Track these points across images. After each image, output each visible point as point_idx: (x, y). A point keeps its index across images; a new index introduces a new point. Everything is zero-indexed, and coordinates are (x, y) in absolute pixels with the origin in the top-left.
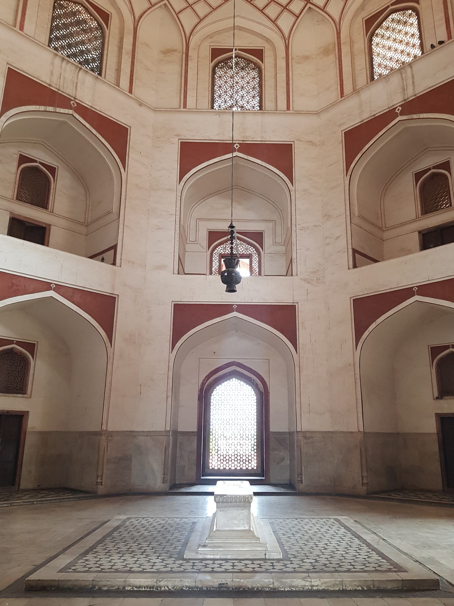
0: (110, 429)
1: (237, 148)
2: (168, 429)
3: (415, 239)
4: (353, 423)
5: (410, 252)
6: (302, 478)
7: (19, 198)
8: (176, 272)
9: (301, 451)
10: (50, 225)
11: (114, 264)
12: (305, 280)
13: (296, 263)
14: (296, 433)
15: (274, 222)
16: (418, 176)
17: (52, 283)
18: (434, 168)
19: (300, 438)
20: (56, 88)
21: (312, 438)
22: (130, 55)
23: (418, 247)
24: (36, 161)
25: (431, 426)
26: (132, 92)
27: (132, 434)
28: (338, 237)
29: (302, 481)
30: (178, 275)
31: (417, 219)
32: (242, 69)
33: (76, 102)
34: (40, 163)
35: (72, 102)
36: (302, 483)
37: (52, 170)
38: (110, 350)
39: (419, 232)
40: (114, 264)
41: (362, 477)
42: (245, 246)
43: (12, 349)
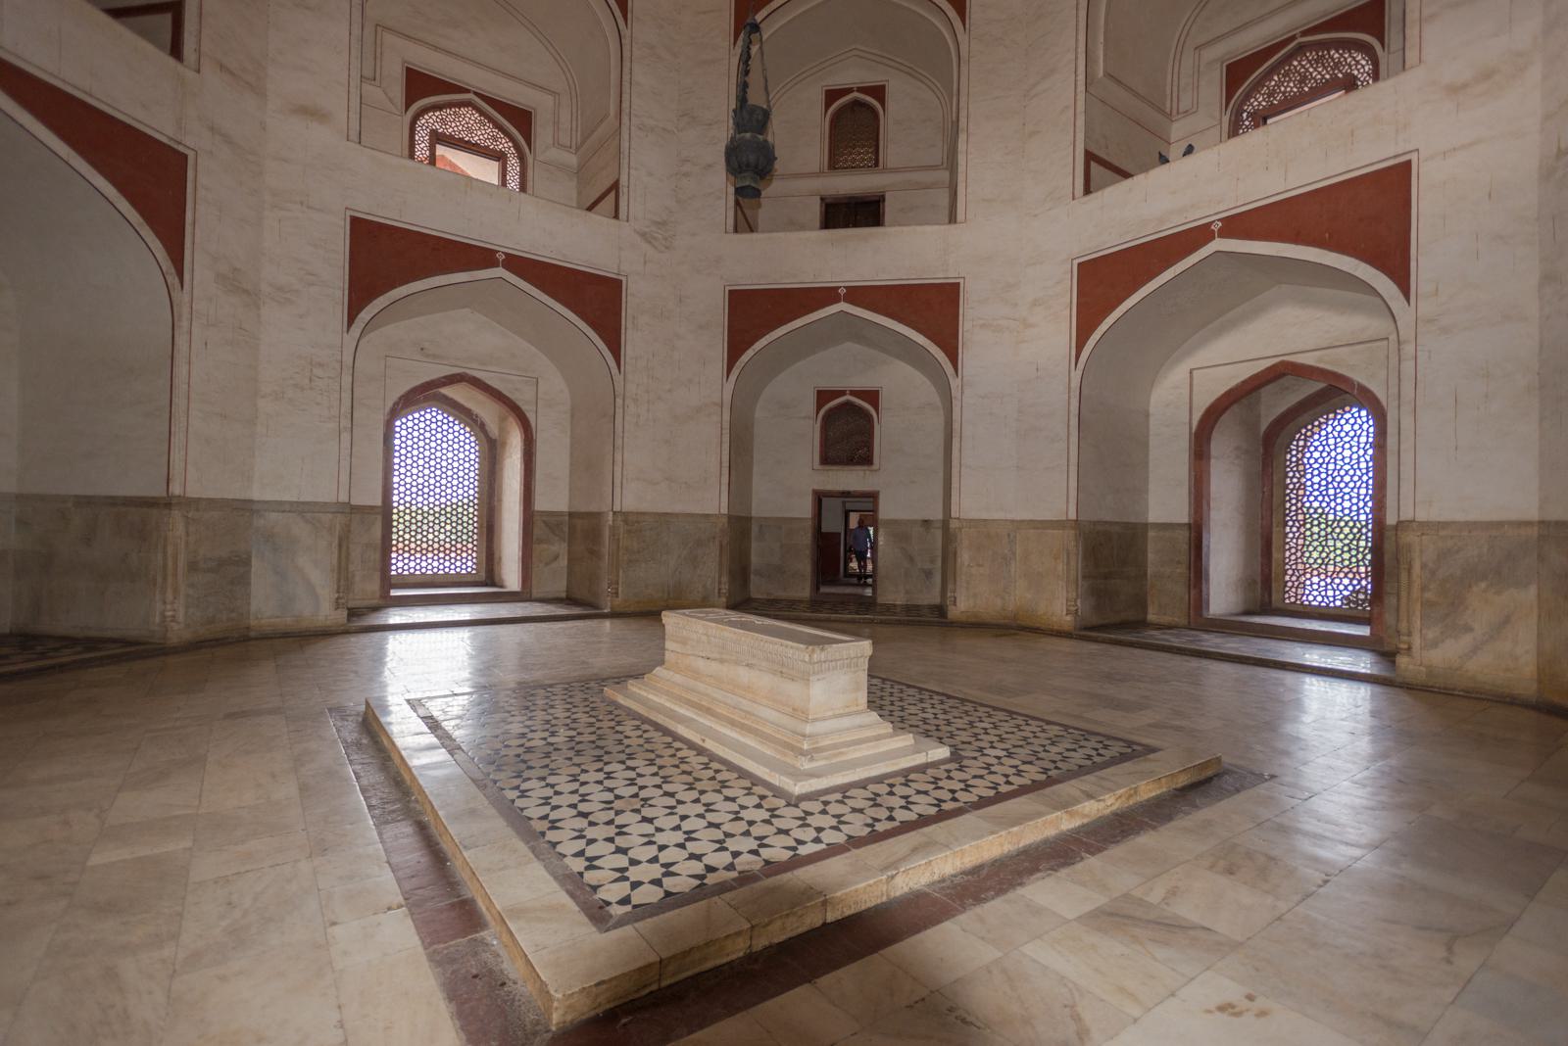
0: (188, 495)
2: (343, 498)
3: (815, 210)
4: (714, 501)
5: (802, 228)
6: (617, 589)
9: (618, 547)
12: (643, 235)
13: (626, 197)
14: (611, 513)
16: (832, 95)
18: (861, 90)
19: (619, 522)
21: (638, 522)
23: (818, 224)
25: (804, 509)
27: (246, 508)
28: (710, 166)
29: (617, 593)
31: (819, 174)
36: (617, 597)
39: (822, 199)
41: (720, 583)
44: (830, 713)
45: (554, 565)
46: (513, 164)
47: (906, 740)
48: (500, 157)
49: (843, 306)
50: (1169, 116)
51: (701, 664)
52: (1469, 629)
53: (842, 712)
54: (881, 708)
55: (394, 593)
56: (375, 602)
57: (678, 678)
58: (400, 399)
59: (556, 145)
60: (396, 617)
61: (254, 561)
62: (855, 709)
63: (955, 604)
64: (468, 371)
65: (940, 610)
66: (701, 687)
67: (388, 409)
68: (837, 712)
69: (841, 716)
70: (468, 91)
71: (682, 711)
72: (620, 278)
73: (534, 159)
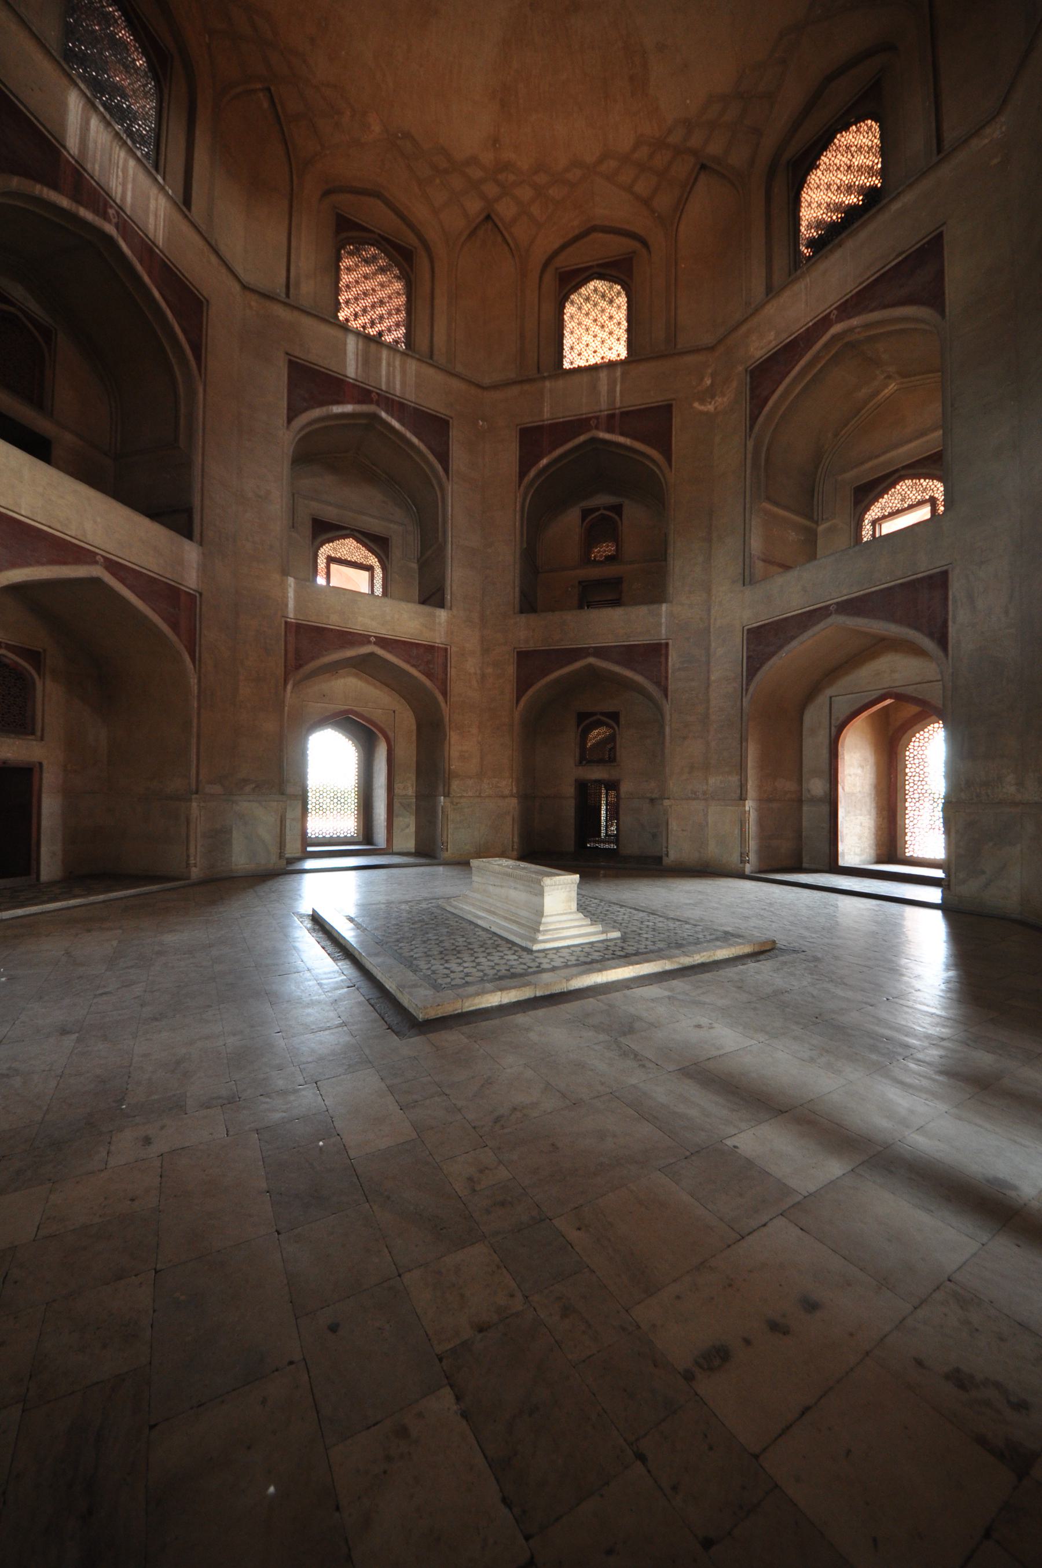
18: (605, 508)
32: (382, 270)
45: (407, 831)
46: (378, 573)
47: (599, 928)
48: (369, 568)
49: (591, 660)
50: (817, 523)
51: (491, 888)
52: (983, 872)
54: (603, 920)
55: (310, 849)
56: (298, 855)
57: (479, 896)
60: (309, 864)
61: (234, 832)
63: (667, 855)
64: (355, 708)
65: (659, 860)
66: (491, 901)
71: (480, 913)
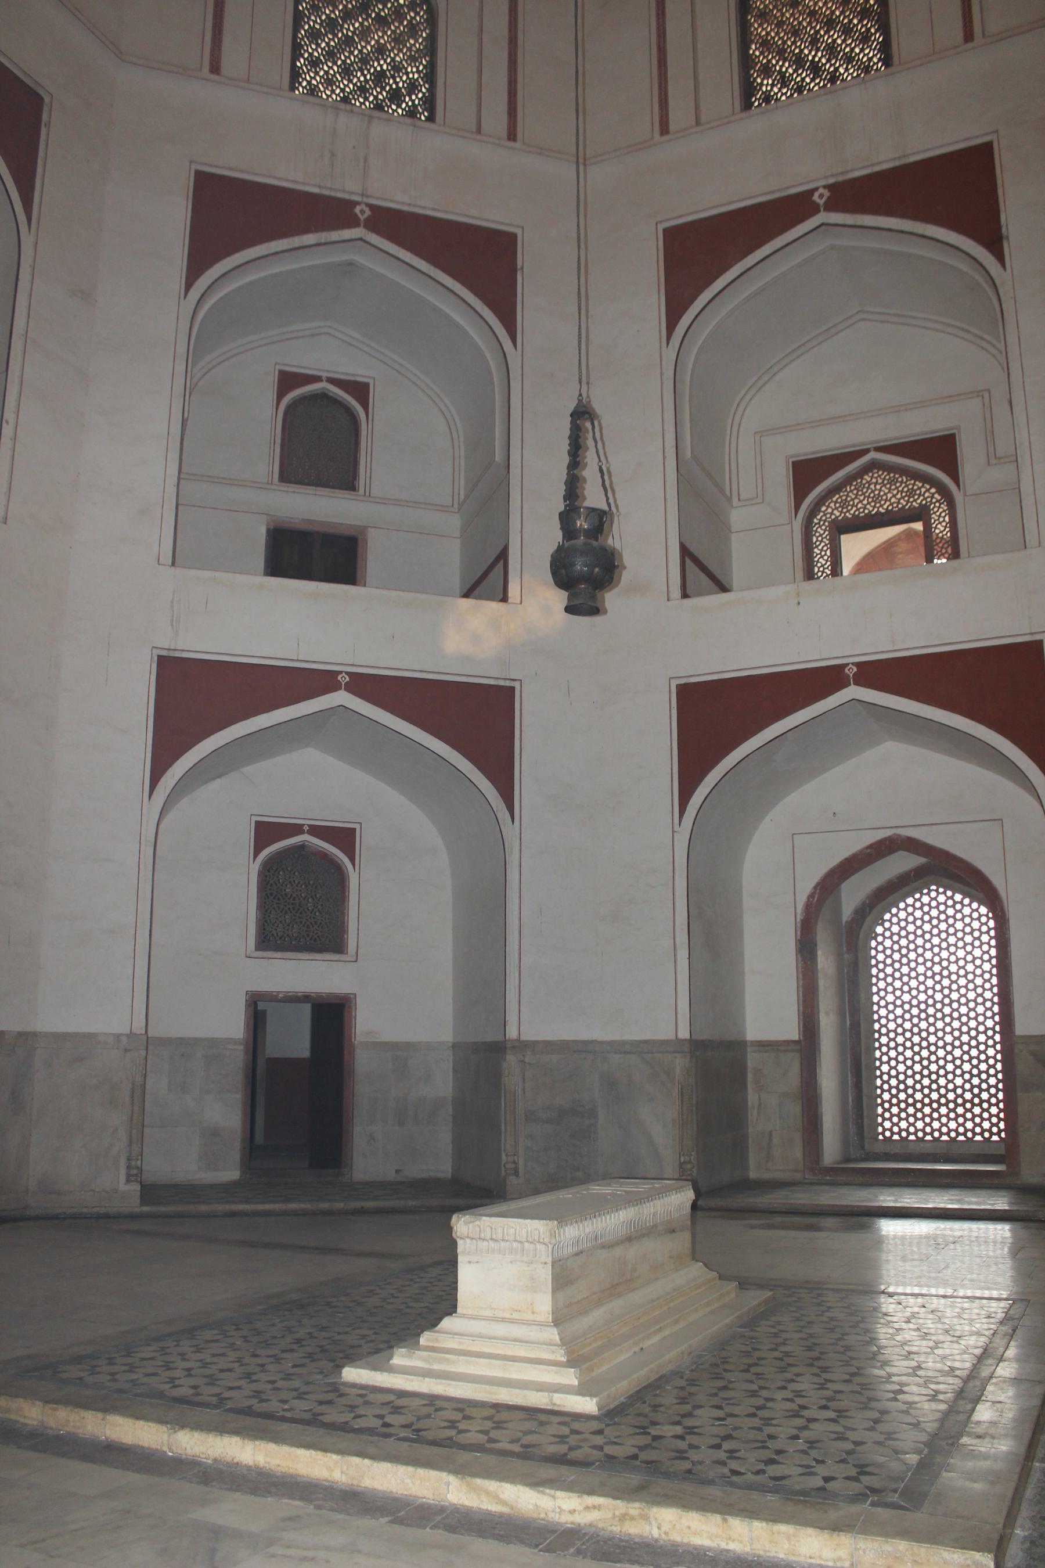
0: (523, 1038)
1: (821, 202)
7: (287, 476)
8: (676, 592)
10: (363, 530)
11: (504, 599)
15: (986, 395)
17: (341, 672)
20: (314, 186)
22: (505, 44)
24: (317, 379)
26: (515, 135)
30: (686, 601)
33: (367, 205)
34: (331, 381)
35: (357, 210)
37: (360, 390)
38: (510, 831)
40: (504, 599)
42: (905, 484)
43: (302, 847)
44: (489, 1313)
47: (570, 1377)
48: (921, 514)
53: (507, 1315)
58: (815, 888)
59: (993, 461)
62: (531, 1317)
67: (800, 906)
68: (500, 1314)
69: (503, 1320)
70: (866, 451)
72: (1037, 637)
73: (965, 495)
